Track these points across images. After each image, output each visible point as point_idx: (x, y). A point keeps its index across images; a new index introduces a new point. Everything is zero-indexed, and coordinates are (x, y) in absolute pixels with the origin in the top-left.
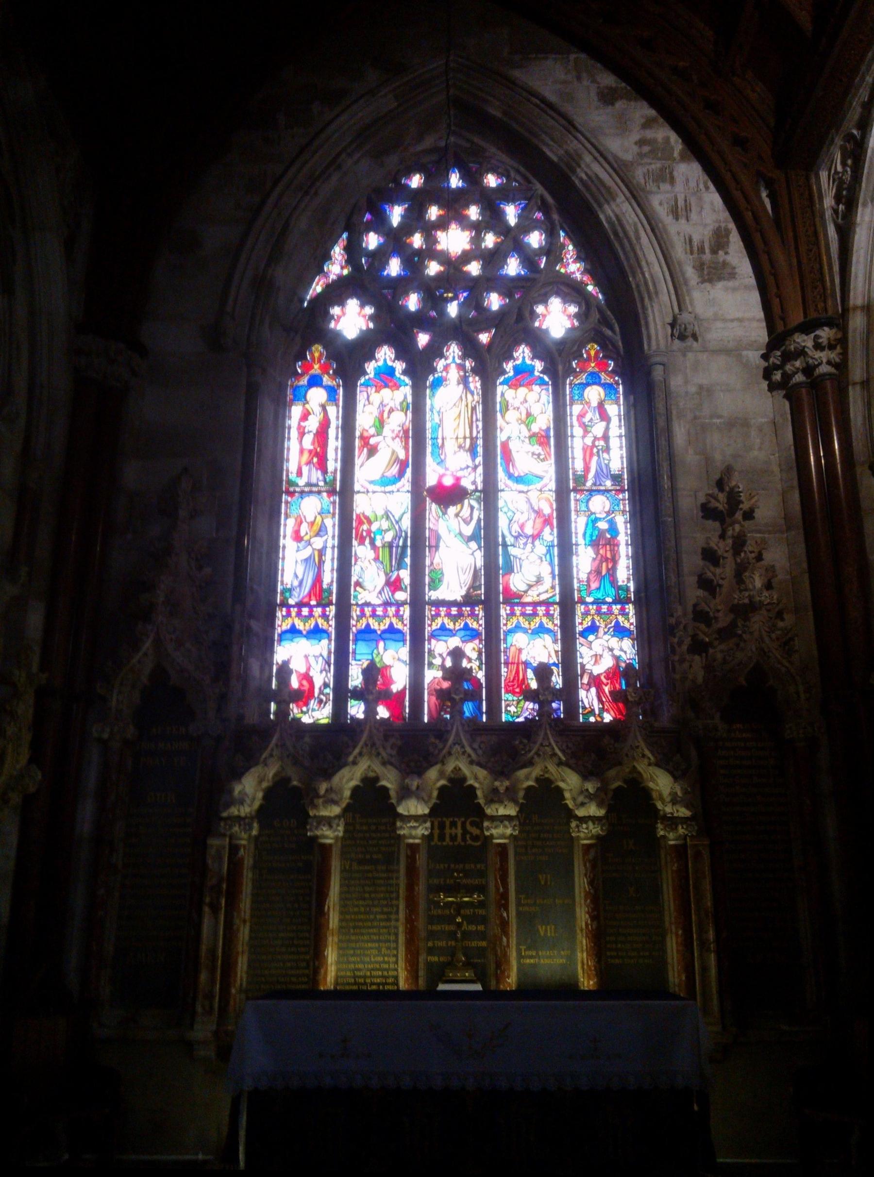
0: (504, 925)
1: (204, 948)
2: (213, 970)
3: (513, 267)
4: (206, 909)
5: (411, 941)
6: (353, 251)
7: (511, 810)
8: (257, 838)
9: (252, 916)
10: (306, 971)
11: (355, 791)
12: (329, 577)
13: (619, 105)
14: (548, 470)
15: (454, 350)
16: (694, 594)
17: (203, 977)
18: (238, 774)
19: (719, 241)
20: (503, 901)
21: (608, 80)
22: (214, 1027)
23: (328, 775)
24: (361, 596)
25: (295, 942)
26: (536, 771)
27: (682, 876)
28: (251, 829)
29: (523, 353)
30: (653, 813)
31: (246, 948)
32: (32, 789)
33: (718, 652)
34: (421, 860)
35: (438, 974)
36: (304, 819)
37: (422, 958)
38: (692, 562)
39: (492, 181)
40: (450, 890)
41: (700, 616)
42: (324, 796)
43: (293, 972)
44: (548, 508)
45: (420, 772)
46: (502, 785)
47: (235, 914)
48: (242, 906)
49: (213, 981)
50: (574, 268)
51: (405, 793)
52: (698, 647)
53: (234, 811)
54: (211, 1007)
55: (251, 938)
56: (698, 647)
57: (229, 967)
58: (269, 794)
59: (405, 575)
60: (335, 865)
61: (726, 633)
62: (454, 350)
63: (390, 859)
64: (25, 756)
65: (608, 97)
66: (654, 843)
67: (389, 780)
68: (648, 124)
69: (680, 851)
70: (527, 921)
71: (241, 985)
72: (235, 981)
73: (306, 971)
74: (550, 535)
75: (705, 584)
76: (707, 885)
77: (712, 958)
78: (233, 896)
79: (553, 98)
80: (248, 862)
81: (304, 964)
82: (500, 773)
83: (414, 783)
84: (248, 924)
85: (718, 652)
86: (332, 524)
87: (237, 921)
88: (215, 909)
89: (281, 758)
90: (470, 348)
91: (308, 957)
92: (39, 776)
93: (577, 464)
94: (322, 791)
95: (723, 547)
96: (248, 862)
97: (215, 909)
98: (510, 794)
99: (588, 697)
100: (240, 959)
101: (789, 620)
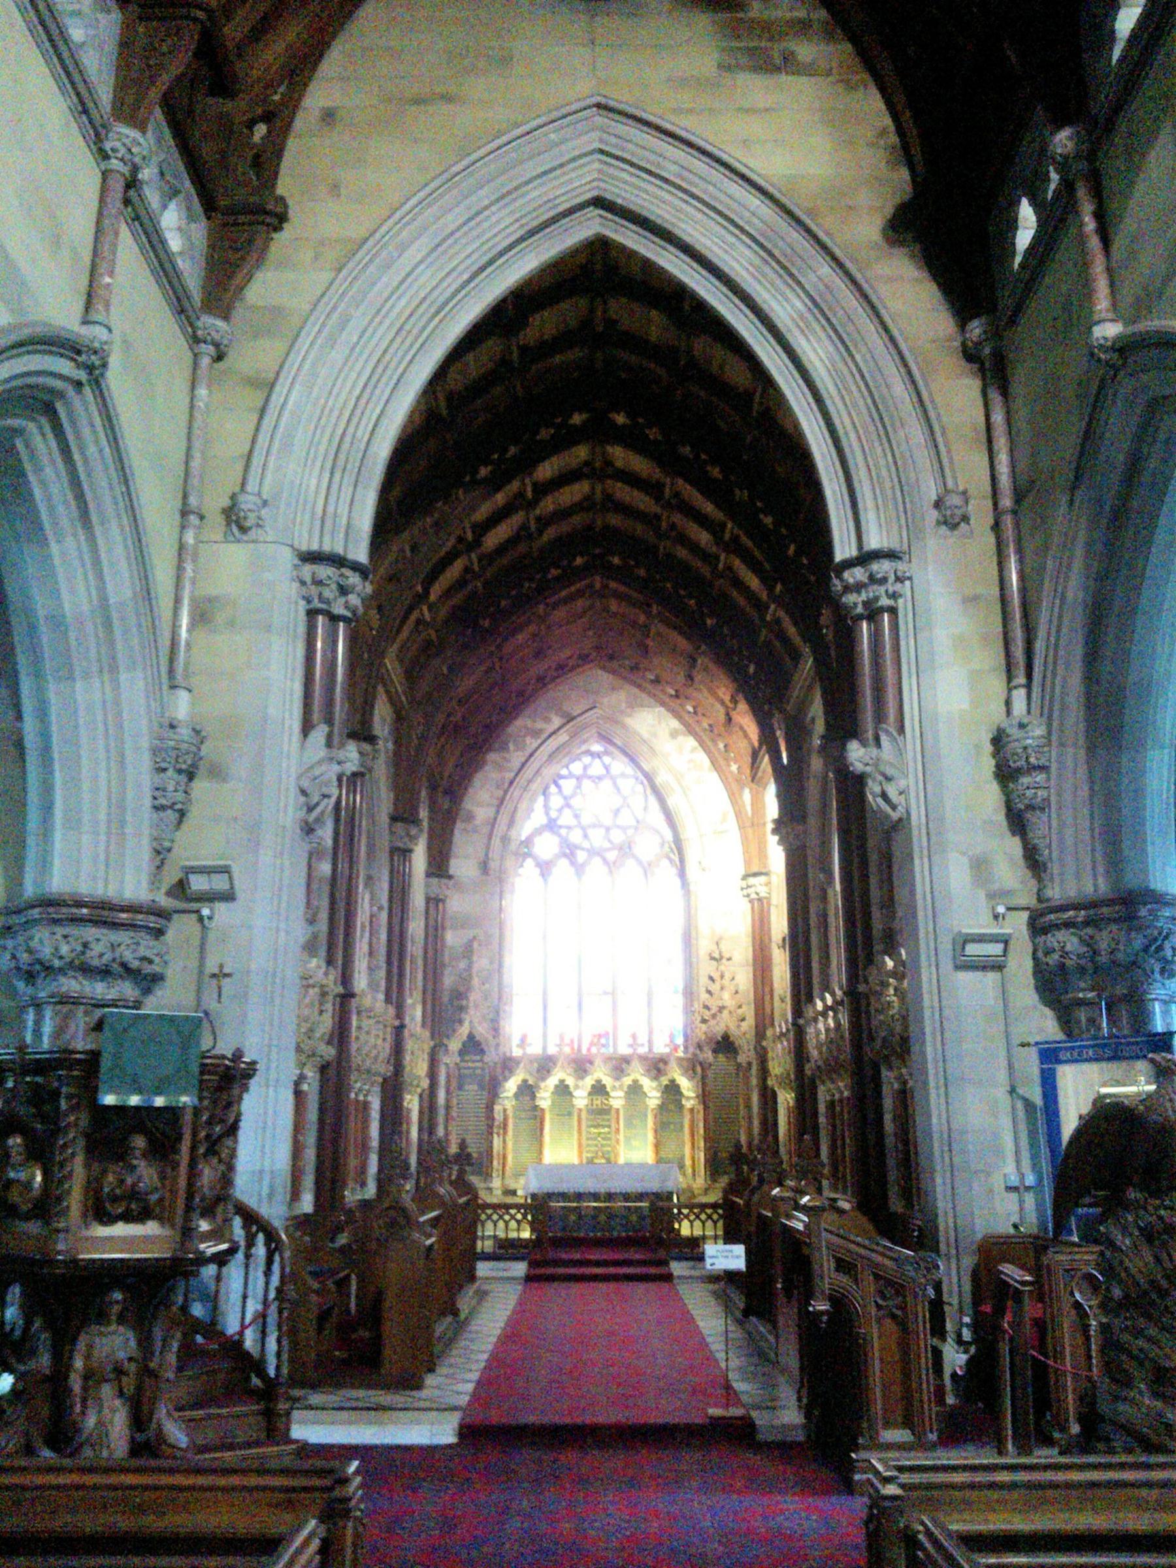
0: (618, 1141)
5: (580, 1146)
7: (621, 1094)
11: (556, 1087)
13: (681, 738)
16: (704, 996)
18: (506, 1079)
20: (618, 1130)
21: (675, 724)
23: (543, 1079)
26: (632, 1077)
27: (692, 1121)
30: (681, 1094)
33: (712, 1022)
34: (584, 1115)
35: (590, 1161)
36: (533, 1097)
37: (585, 1155)
38: (704, 981)
40: (595, 1127)
41: (707, 1007)
45: (582, 1078)
46: (617, 1084)
51: (577, 1087)
52: (704, 1021)
56: (704, 1021)
57: (505, 1157)
58: (519, 1087)
60: (548, 1117)
61: (714, 1016)
63: (570, 1114)
65: (674, 734)
66: (681, 1107)
67: (570, 1081)
68: (693, 750)
69: (692, 1110)
70: (628, 1139)
75: (709, 992)
76: (701, 1125)
77: (702, 1155)
79: (645, 735)
82: (617, 1079)
83: (580, 1083)
85: (712, 1022)
95: (716, 976)
98: (621, 1087)
101: (744, 1008)
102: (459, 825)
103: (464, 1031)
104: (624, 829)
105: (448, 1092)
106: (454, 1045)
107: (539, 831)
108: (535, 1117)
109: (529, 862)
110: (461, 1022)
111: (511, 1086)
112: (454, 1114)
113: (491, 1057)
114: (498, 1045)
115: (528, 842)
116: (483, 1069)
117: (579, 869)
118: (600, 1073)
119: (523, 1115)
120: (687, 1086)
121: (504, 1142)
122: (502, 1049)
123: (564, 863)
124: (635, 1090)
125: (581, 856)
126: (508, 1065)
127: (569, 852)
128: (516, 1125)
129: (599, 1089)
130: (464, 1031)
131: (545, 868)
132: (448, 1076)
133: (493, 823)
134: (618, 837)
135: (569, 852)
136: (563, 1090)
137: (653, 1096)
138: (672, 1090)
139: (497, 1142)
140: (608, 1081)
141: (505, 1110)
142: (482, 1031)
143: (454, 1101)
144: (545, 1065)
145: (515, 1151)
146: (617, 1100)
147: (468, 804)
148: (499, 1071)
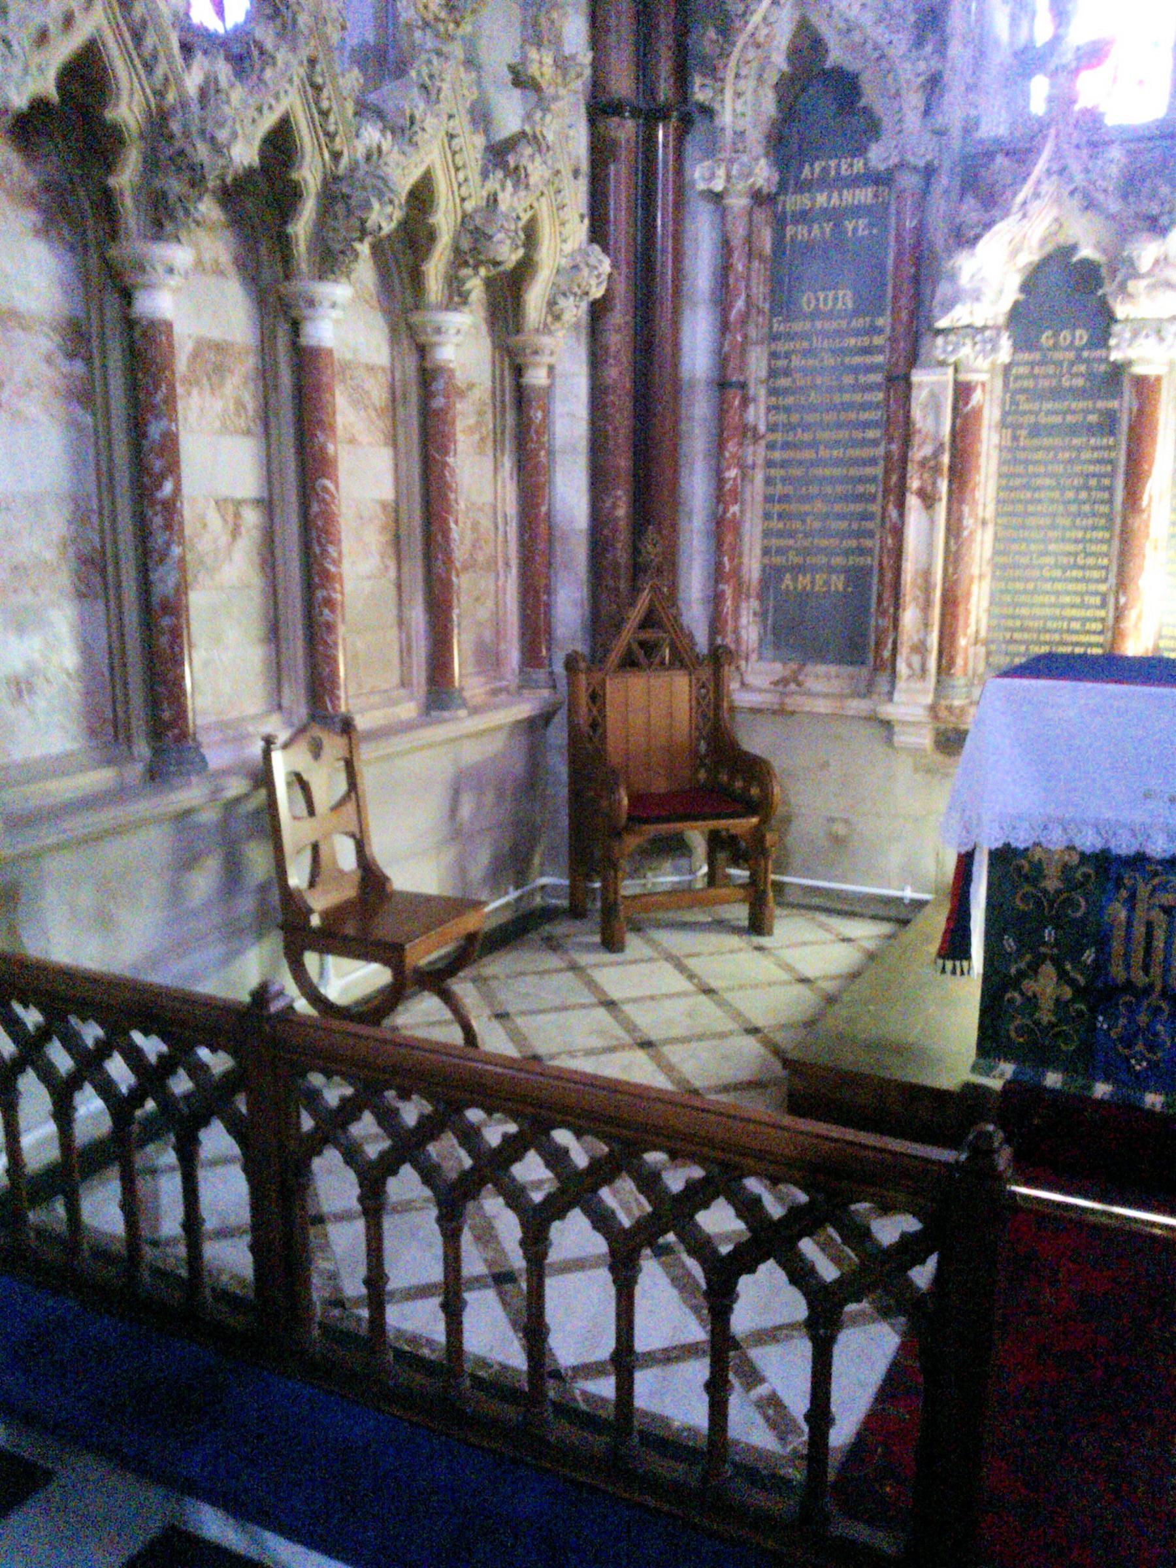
1: (910, 568)
2: (927, 606)
4: (913, 501)
8: (1007, 368)
9: (998, 514)
10: (1101, 613)
17: (910, 617)
18: (964, 238)
22: (929, 699)
25: (1080, 561)
28: (995, 349)
31: (987, 569)
32: (597, 293)
42: (1150, 273)
43: (1074, 612)
47: (966, 509)
48: (978, 494)
49: (926, 625)
53: (958, 315)
54: (924, 669)
55: (996, 552)
64: (579, 231)
71: (977, 632)
72: (967, 625)
73: (1101, 613)
78: (960, 473)
80: (991, 415)
81: (1097, 600)
84: (990, 530)
87: (968, 522)
88: (928, 499)
89: (1058, 200)
91: (1103, 588)
92: (606, 266)
94: (1144, 265)
96: (991, 415)
97: (928, 499)
100: (975, 588)
105: (724, 327)
108: (1109, 423)
112: (757, 415)
114: (934, 84)
116: (876, 214)
119: (1048, 412)
121: (954, 529)
122: (953, 112)
128: (1012, 456)
132: (725, 246)
141: (963, 391)
143: (757, 363)
145: (1003, 567)
148: (939, 205)
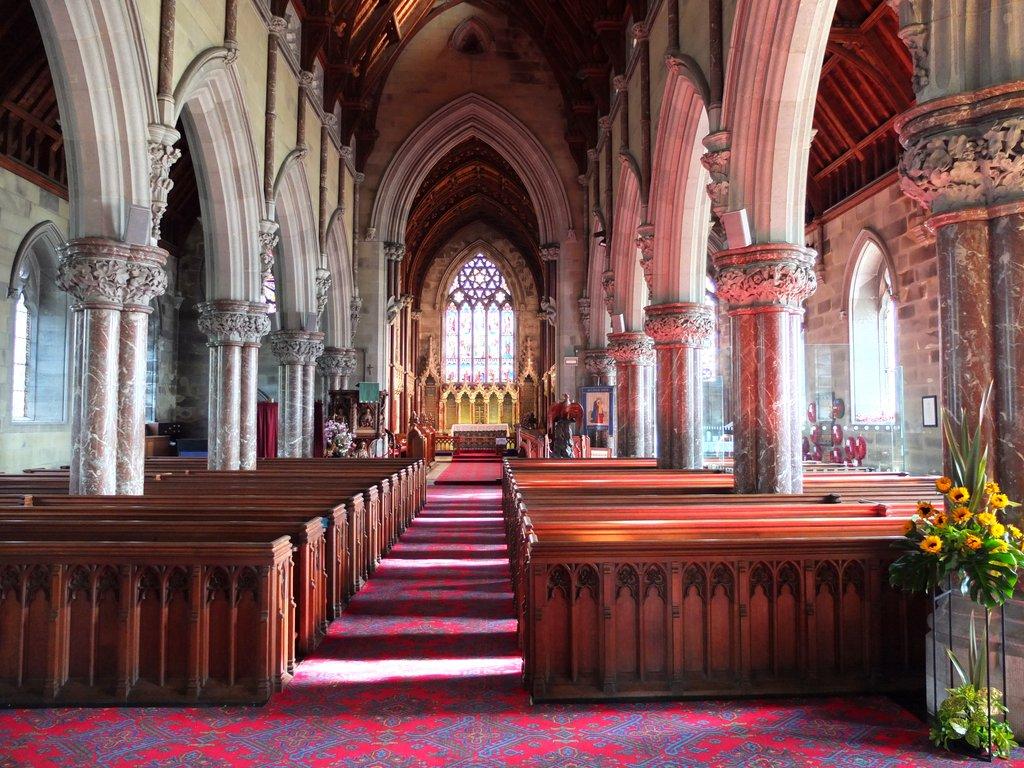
3: (492, 286)
6: (459, 281)
12: (456, 354)
14: (498, 331)
15: (480, 304)
19: (531, 287)
24: (461, 357)
29: (493, 305)
39: (488, 264)
44: (498, 340)
50: (504, 286)
59: (470, 353)
62: (480, 304)
65: (511, 251)
68: (519, 258)
70: (491, 415)
74: (498, 345)
86: (456, 342)
90: (483, 304)
93: (503, 331)
99: (503, 377)
102: (424, 289)
103: (427, 374)
104: (491, 290)
106: (424, 379)
107: (455, 291)
109: (452, 304)
110: (426, 369)
111: (445, 395)
113: (437, 385)
115: (451, 296)
117: (473, 307)
118: (480, 389)
120: (515, 395)
123: (466, 305)
124: (493, 396)
125: (473, 301)
126: (444, 387)
127: (468, 298)
129: (479, 396)
130: (427, 374)
131: (459, 306)
133: (437, 288)
134: (488, 293)
135: (468, 298)
136: (465, 396)
137: (500, 396)
138: (508, 396)
139: (441, 416)
140: (483, 393)
142: (434, 373)
144: (459, 386)
146: (487, 400)
147: (427, 280)
